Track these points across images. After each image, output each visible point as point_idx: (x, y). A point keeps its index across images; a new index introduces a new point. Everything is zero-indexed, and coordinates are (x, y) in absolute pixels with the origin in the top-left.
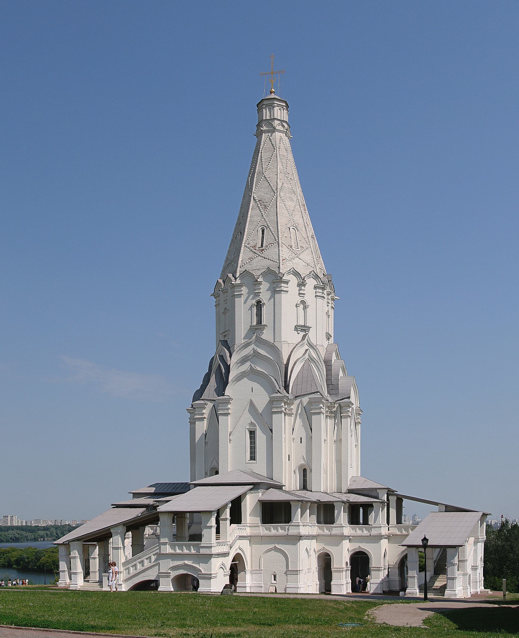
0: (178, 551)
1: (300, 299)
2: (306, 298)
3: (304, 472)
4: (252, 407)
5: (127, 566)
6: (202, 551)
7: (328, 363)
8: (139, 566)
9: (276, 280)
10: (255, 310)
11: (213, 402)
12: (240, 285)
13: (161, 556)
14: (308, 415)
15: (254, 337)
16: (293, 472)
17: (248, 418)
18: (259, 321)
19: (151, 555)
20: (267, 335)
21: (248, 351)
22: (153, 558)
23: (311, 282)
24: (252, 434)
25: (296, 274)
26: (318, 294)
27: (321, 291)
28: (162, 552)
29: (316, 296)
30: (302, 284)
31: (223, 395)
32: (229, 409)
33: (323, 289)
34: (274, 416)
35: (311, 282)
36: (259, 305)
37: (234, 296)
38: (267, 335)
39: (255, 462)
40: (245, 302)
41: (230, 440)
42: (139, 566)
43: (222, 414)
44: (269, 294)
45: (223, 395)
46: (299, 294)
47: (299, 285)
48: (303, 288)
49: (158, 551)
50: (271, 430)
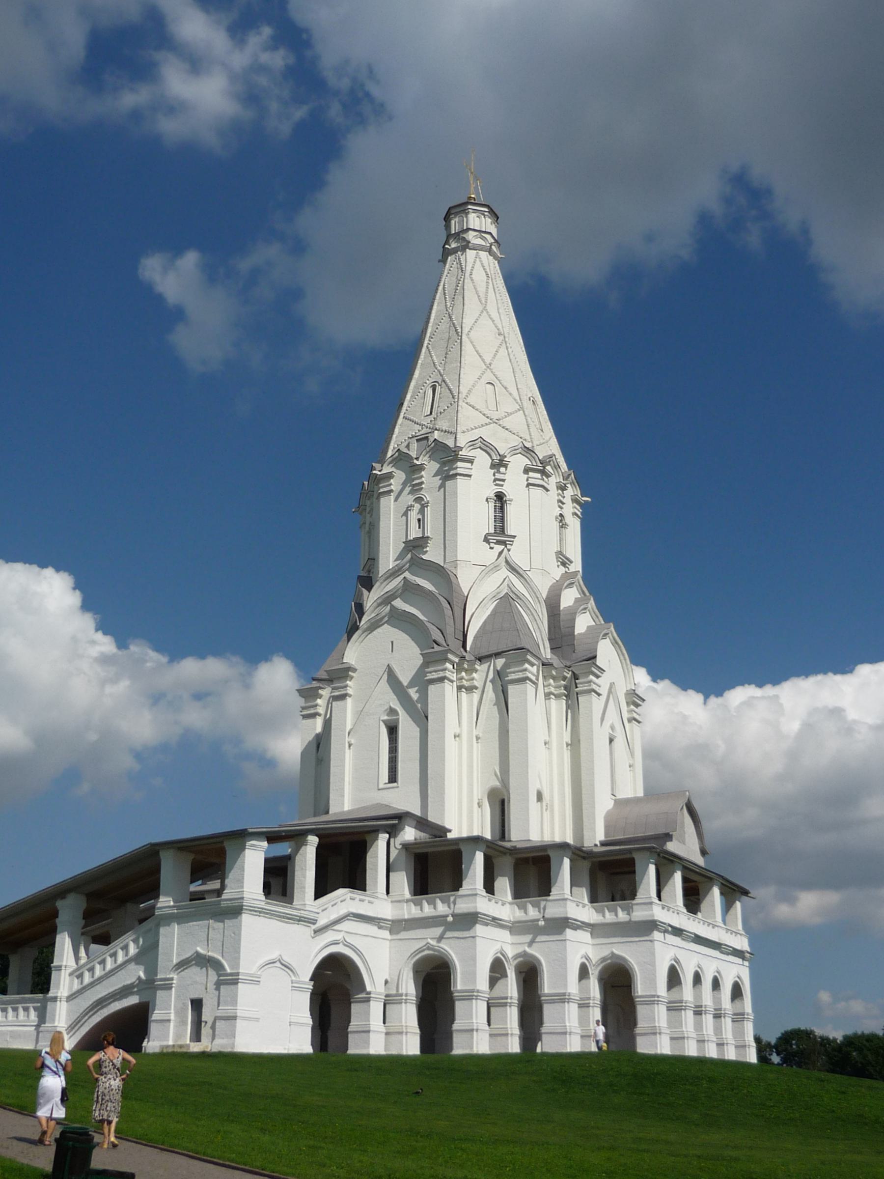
2: (506, 489)
3: (500, 805)
7: (552, 604)
9: (448, 458)
12: (389, 476)
15: (409, 556)
16: (476, 806)
20: (432, 554)
23: (517, 463)
24: (393, 731)
25: (486, 447)
26: (531, 481)
27: (538, 475)
29: (528, 485)
30: (499, 464)
33: (544, 473)
35: (517, 463)
38: (432, 554)
39: (395, 785)
41: (350, 745)
44: (437, 481)
46: (495, 480)
47: (493, 466)
48: (502, 469)
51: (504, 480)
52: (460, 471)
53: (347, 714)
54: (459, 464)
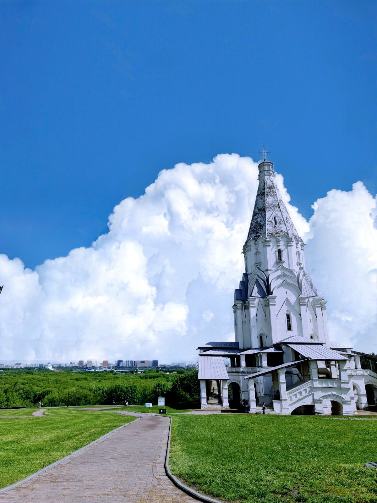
0: (325, 386)
1: (296, 250)
4: (287, 301)
5: (290, 395)
6: (343, 386)
8: (298, 396)
10: (277, 253)
11: (259, 298)
13: (313, 388)
14: (314, 307)
17: (285, 308)
18: (280, 259)
19: (307, 387)
20: (285, 265)
21: (279, 273)
22: (308, 390)
24: (288, 316)
28: (314, 386)
29: (302, 250)
31: (272, 294)
32: (275, 302)
34: (301, 307)
35: (300, 243)
36: (280, 251)
37: (265, 246)
40: (272, 249)
41: (277, 319)
42: (298, 396)
43: (271, 305)
45: (272, 294)
46: (297, 248)
49: (311, 385)
50: (300, 315)
51: (298, 248)
52: (292, 245)
53: (273, 310)
54: (291, 242)
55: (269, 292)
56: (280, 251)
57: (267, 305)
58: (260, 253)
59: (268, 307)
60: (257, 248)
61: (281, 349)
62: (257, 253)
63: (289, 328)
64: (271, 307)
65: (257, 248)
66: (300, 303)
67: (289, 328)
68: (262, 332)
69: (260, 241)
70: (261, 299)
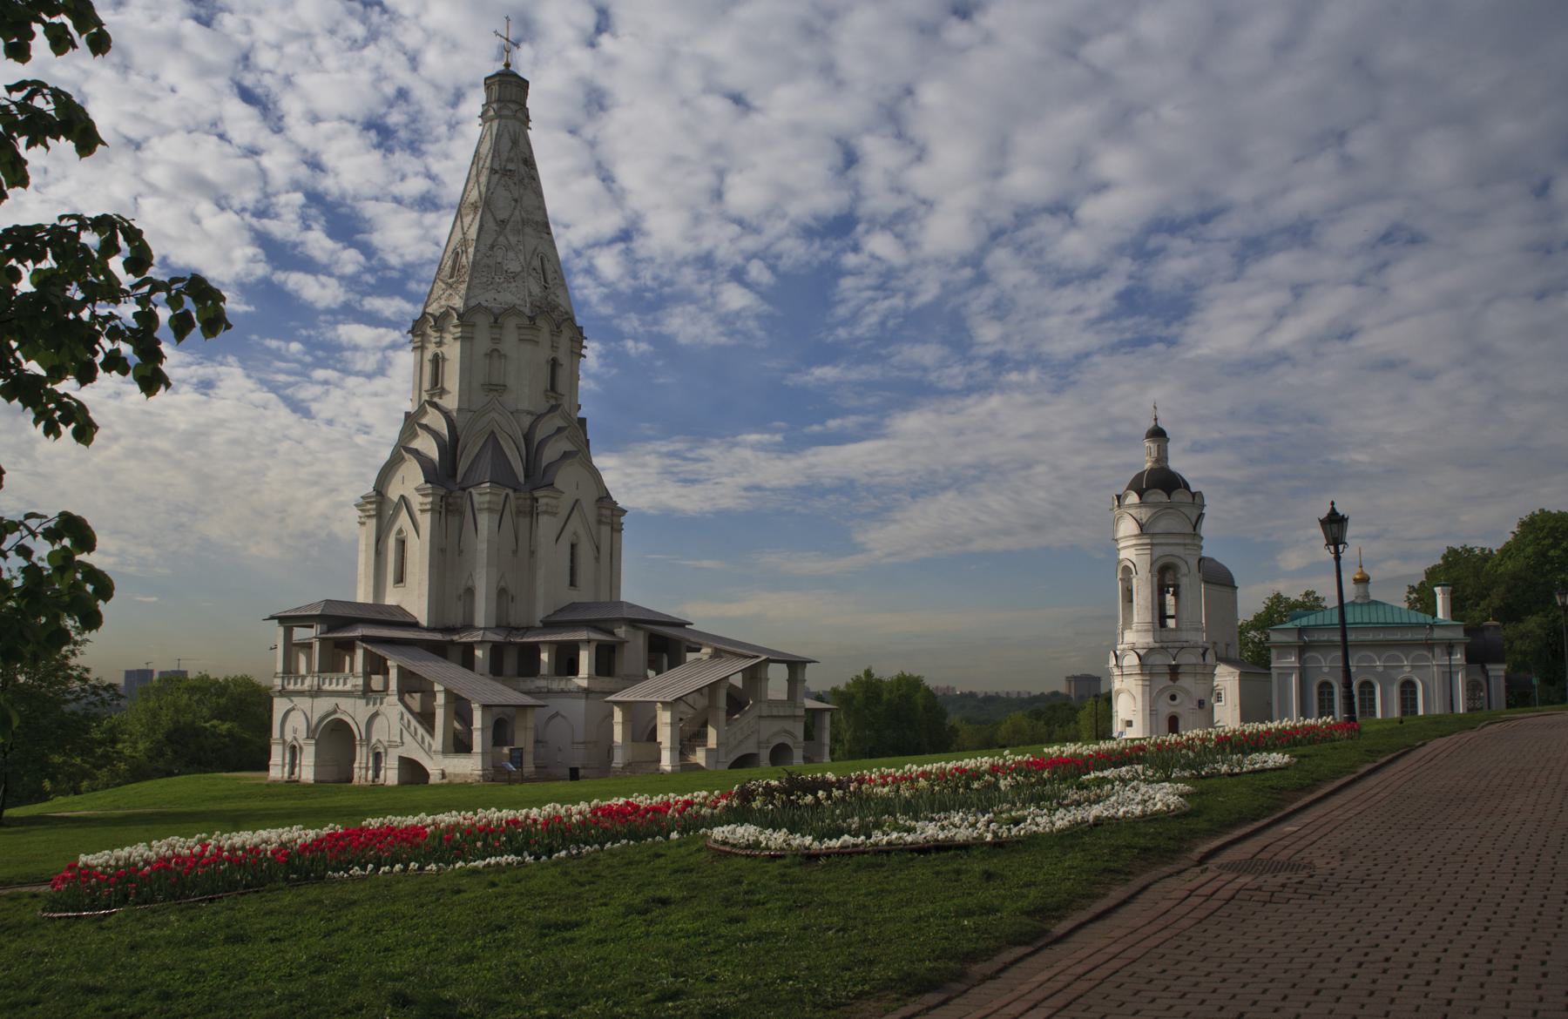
0: (775, 713)
18: (553, 387)
24: (573, 546)
36: (554, 364)
53: (546, 526)
55: (537, 477)
56: (554, 364)
57: (532, 513)
58: (502, 356)
59: (528, 520)
60: (496, 340)
61: (613, 634)
62: (494, 354)
63: (573, 583)
64: (543, 519)
65: (496, 340)
66: (600, 515)
67: (573, 583)
68: (503, 584)
69: (511, 323)
70: (510, 492)
